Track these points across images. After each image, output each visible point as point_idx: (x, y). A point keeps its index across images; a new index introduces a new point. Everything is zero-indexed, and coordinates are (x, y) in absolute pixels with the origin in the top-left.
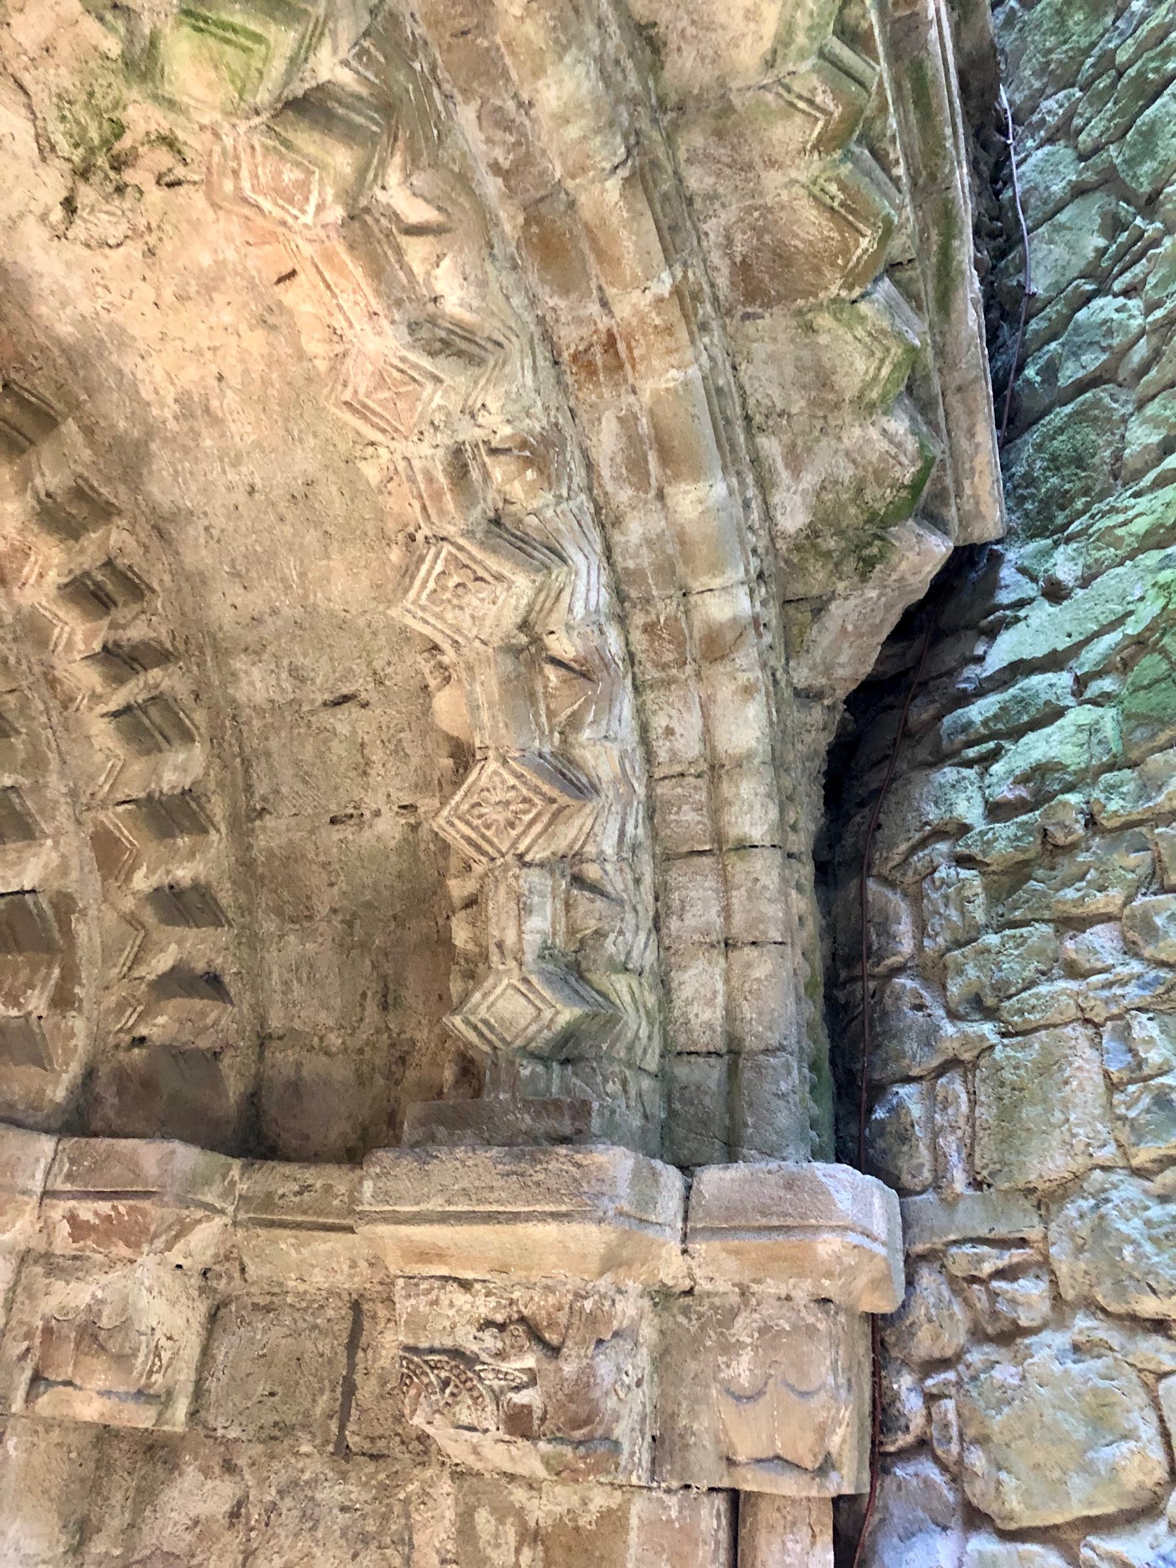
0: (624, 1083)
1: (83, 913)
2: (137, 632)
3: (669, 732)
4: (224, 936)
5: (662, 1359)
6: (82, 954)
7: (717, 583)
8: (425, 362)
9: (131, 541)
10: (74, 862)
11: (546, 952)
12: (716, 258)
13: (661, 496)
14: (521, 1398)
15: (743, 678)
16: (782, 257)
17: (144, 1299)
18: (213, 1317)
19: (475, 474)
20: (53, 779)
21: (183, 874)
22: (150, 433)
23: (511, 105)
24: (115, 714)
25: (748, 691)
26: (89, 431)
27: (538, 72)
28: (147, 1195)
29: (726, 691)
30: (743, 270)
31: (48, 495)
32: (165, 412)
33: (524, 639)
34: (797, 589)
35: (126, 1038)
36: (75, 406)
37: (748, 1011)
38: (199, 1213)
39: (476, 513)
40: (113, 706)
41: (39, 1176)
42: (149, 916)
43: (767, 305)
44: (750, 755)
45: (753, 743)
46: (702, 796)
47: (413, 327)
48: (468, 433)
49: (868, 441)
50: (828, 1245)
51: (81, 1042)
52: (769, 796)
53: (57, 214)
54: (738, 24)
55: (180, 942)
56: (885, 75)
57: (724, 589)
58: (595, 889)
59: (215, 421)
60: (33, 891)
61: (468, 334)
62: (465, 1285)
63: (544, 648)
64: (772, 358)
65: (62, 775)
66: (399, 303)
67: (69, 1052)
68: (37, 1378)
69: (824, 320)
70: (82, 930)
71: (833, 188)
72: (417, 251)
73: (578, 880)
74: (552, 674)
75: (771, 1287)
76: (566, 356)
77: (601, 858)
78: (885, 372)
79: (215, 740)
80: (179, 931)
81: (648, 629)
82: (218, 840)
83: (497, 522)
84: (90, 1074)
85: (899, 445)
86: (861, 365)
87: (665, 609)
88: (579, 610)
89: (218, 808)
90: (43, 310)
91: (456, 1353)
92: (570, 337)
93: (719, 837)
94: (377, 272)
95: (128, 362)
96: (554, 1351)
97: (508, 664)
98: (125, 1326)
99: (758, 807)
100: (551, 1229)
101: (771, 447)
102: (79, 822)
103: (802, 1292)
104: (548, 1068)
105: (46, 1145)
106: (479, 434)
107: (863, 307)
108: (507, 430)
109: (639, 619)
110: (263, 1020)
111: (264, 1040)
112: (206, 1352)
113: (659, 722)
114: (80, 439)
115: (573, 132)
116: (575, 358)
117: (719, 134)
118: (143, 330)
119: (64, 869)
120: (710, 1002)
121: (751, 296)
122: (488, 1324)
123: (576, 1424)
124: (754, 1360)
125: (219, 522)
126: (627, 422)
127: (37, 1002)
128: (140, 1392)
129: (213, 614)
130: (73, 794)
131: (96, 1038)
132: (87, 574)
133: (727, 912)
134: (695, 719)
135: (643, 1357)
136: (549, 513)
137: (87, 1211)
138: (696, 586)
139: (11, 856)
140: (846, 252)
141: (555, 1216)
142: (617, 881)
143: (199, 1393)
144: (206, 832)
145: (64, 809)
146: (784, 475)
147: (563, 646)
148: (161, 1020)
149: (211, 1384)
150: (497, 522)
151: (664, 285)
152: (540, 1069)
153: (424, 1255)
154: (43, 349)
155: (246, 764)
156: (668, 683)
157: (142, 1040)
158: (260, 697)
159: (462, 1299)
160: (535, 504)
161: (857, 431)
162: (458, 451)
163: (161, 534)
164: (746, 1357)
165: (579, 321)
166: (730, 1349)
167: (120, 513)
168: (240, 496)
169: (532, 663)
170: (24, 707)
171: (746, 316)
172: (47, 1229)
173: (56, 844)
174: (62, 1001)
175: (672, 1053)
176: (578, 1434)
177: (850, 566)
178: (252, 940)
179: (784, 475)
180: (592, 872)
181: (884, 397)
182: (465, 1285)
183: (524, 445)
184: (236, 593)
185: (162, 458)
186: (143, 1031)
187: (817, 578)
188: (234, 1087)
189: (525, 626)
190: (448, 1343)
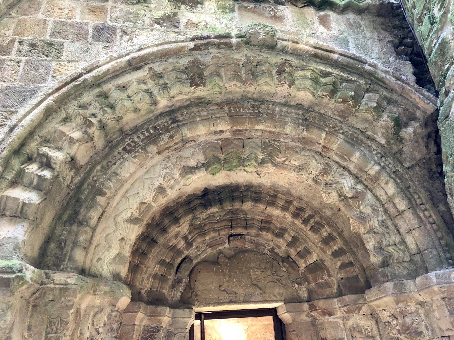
0: (398, 267)
1: (325, 261)
2: (306, 215)
3: (380, 196)
4: (348, 255)
5: (427, 315)
6: (328, 267)
7: (368, 168)
8: (299, 174)
9: (298, 204)
10: (319, 253)
11: (375, 248)
12: (335, 117)
13: (350, 161)
14: (398, 328)
15: (384, 181)
16: (342, 111)
17: (359, 322)
18: (377, 322)
19: (318, 180)
20: (309, 243)
21: (336, 248)
22: (288, 189)
23: (285, 136)
24: (310, 230)
25: (387, 183)
26: (282, 194)
27: (284, 132)
28: (348, 305)
29: (383, 185)
30: (340, 116)
31: (282, 205)
32: (287, 186)
33: (342, 198)
34: (394, 151)
35: (340, 279)
36: (278, 192)
37: (419, 244)
38: (361, 305)
39: (322, 185)
40: (309, 229)
41: (337, 305)
42: (332, 258)
43: (348, 117)
44: (394, 194)
45: (394, 192)
46: (392, 205)
47: (294, 171)
48: (312, 176)
49: (382, 124)
50: (436, 288)
51: (335, 281)
52: (403, 199)
53: (258, 176)
54: (306, 97)
55: (340, 260)
56: (337, 73)
57: (370, 169)
58: (377, 233)
59: (293, 183)
60: (317, 260)
61: (302, 165)
62: (384, 310)
63: (347, 197)
64: (357, 122)
65: (310, 241)
66: (290, 169)
67: (334, 284)
68: (352, 337)
69: (357, 114)
70: (326, 263)
71: (339, 100)
72: (287, 163)
73: (374, 233)
74: (350, 201)
75: (435, 298)
76: (321, 152)
77: (376, 228)
78: (374, 113)
79: (329, 224)
80: (338, 259)
81: (366, 180)
82: (338, 240)
83: (326, 184)
84: (339, 286)
85: (387, 121)
86: (369, 115)
87: (365, 176)
88: (347, 189)
89: (335, 234)
90: (266, 184)
91: (388, 322)
92: (319, 150)
93: (398, 211)
94: (285, 169)
95: (278, 183)
96: (397, 319)
97: (342, 203)
98: (358, 326)
99: (401, 203)
100: (385, 299)
101: (369, 133)
102: (317, 247)
103: (439, 297)
104: (384, 268)
105: (336, 300)
106: (314, 175)
107: (361, 108)
108: (317, 173)
109: (363, 180)
110: (363, 267)
111: (364, 270)
112: (378, 328)
113: (378, 195)
114: (281, 195)
115: (294, 133)
116: (322, 151)
117: (318, 106)
118: (276, 179)
119: (318, 255)
120: (412, 244)
121: (345, 118)
122: (390, 316)
123: (406, 330)
124: (438, 312)
125: (305, 194)
126: (336, 154)
127: (326, 277)
128: (367, 337)
129: (315, 205)
130: (314, 243)
131: (337, 280)
132: (294, 212)
133: (407, 225)
134: (382, 191)
135: (423, 316)
136: (332, 178)
137: (345, 309)
138: (366, 170)
139: (309, 258)
140: (349, 105)
141: (385, 296)
142: (381, 230)
143: (380, 335)
144: (335, 240)
145: (313, 246)
146: (375, 136)
147: (349, 195)
148: (342, 274)
149: (381, 333)
150: (326, 184)
151: (324, 135)
152: (383, 269)
153: (378, 306)
154: (269, 188)
155: (336, 224)
156: (374, 188)
157: (342, 278)
158: (330, 214)
159: (385, 313)
160: (329, 179)
161: (379, 124)
162: (313, 179)
163: (300, 199)
164: (437, 312)
165: (318, 148)
166: (434, 311)
167: (293, 201)
168: (304, 190)
169: (347, 201)
170: (299, 234)
171: (347, 120)
172: (343, 313)
173: (315, 252)
174: (329, 276)
175: (412, 255)
176: (407, 332)
177: (398, 143)
178: (354, 254)
179: (375, 136)
180: (375, 230)
181: (378, 116)
182: (384, 310)
183: (321, 173)
184: (315, 202)
185: (293, 191)
186: (341, 277)
187: (395, 149)
188: (362, 280)
189: (340, 196)
190: (387, 321)
